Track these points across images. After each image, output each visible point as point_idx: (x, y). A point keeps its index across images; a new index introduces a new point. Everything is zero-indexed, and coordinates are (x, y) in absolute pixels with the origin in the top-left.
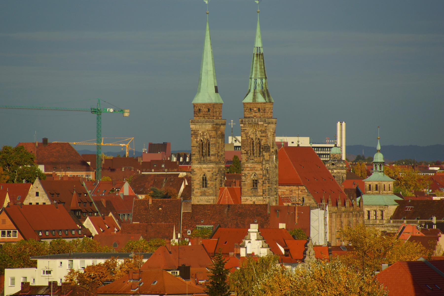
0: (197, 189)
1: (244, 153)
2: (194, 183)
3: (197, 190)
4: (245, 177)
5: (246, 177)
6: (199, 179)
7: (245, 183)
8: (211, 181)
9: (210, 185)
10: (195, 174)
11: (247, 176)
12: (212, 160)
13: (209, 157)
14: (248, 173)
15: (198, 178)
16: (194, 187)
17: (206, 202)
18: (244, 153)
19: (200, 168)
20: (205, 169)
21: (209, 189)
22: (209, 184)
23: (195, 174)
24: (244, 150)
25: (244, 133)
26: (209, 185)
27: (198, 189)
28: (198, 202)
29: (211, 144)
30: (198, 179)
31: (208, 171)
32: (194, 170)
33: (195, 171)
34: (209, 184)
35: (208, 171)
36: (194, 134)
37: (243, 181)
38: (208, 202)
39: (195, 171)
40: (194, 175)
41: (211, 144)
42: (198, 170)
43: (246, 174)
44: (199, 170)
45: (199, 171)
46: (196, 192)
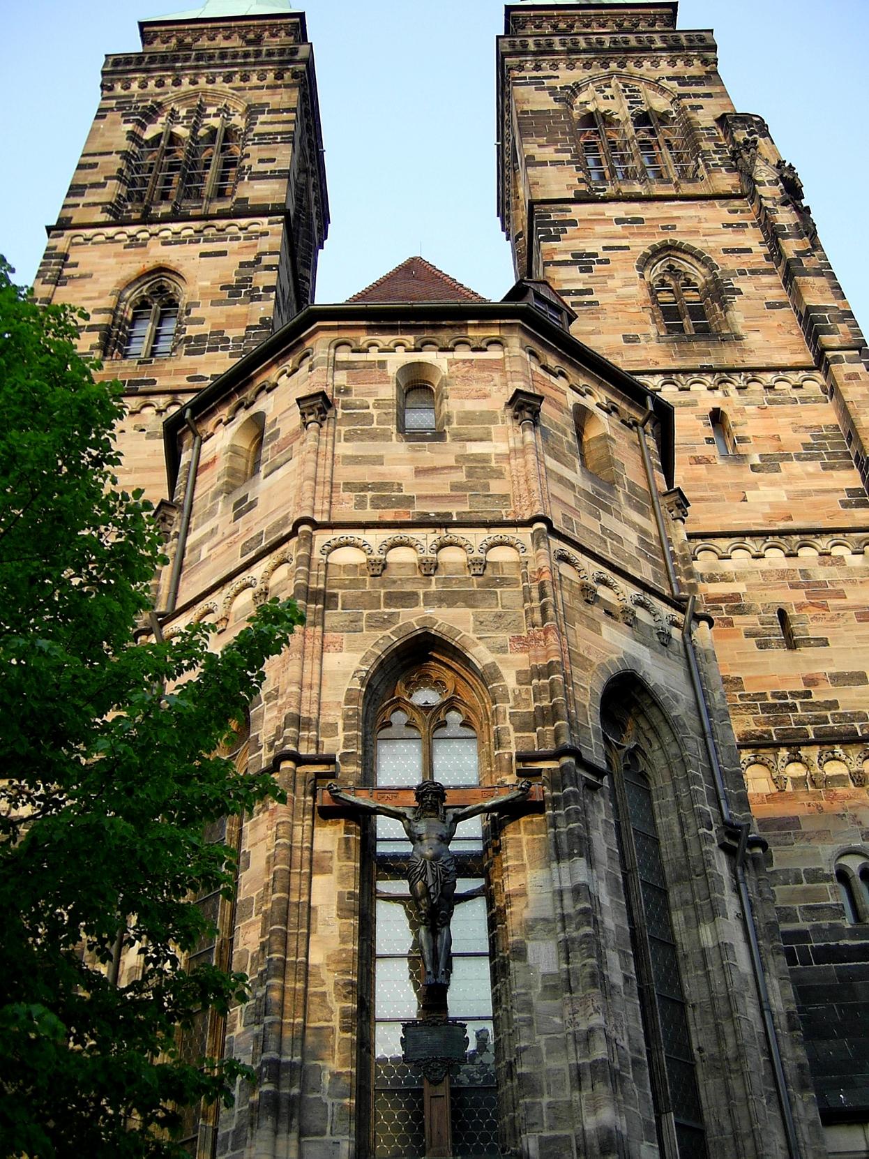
14: (605, 248)
36: (119, 109)
43: (595, 255)
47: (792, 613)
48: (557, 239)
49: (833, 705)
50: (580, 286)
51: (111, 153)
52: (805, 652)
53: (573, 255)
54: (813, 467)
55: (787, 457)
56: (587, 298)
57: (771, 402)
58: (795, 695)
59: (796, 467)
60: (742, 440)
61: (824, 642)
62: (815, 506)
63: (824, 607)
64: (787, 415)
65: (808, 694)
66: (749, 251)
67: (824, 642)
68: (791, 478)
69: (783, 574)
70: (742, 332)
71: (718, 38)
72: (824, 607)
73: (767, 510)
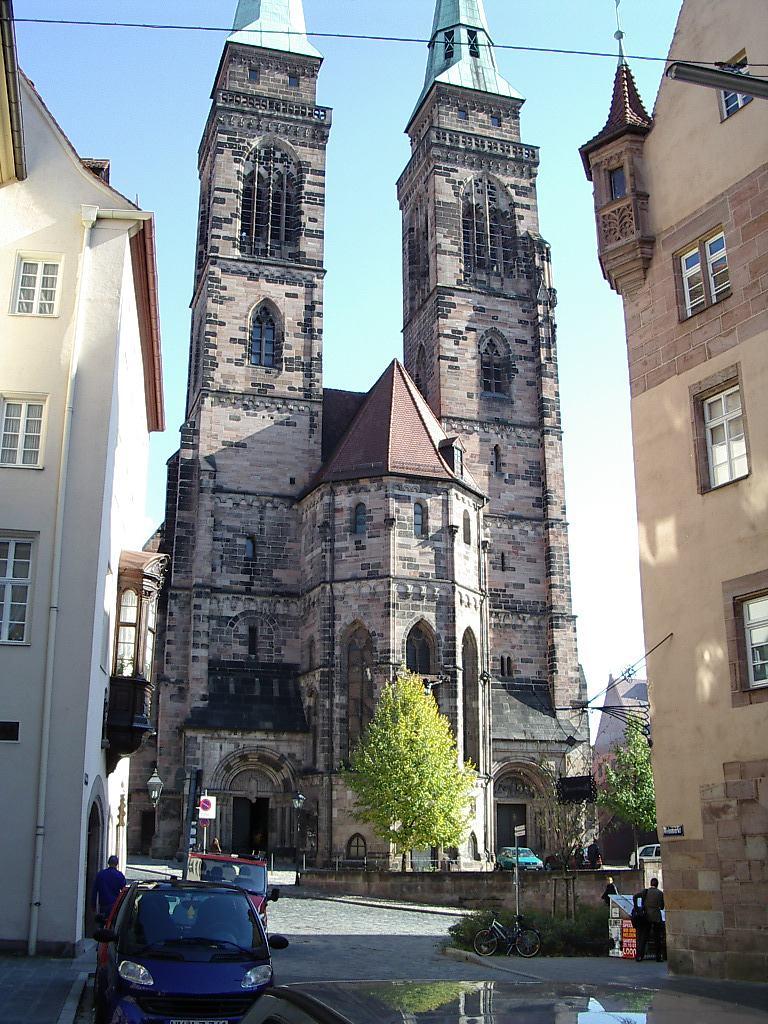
0: (229, 361)
1: (451, 253)
4: (457, 344)
5: (461, 341)
7: (457, 368)
10: (221, 301)
11: (465, 339)
15: (238, 315)
16: (219, 354)
18: (451, 253)
22: (289, 347)
24: (448, 241)
25: (447, 181)
27: (236, 364)
31: (287, 295)
33: (225, 288)
34: (289, 347)
35: (287, 295)
37: (446, 358)
39: (225, 288)
43: (461, 332)
47: (506, 555)
48: (446, 317)
49: (512, 596)
50: (453, 355)
51: (229, 191)
52: (507, 573)
53: (453, 331)
54: (526, 483)
55: (518, 477)
56: (456, 364)
57: (518, 444)
58: (501, 590)
59: (520, 483)
60: (504, 464)
61: (514, 569)
62: (524, 504)
63: (517, 553)
64: (522, 453)
65: (505, 591)
66: (525, 342)
67: (514, 569)
68: (518, 489)
69: (507, 536)
70: (514, 398)
71: (542, 155)
72: (517, 553)
73: (506, 504)
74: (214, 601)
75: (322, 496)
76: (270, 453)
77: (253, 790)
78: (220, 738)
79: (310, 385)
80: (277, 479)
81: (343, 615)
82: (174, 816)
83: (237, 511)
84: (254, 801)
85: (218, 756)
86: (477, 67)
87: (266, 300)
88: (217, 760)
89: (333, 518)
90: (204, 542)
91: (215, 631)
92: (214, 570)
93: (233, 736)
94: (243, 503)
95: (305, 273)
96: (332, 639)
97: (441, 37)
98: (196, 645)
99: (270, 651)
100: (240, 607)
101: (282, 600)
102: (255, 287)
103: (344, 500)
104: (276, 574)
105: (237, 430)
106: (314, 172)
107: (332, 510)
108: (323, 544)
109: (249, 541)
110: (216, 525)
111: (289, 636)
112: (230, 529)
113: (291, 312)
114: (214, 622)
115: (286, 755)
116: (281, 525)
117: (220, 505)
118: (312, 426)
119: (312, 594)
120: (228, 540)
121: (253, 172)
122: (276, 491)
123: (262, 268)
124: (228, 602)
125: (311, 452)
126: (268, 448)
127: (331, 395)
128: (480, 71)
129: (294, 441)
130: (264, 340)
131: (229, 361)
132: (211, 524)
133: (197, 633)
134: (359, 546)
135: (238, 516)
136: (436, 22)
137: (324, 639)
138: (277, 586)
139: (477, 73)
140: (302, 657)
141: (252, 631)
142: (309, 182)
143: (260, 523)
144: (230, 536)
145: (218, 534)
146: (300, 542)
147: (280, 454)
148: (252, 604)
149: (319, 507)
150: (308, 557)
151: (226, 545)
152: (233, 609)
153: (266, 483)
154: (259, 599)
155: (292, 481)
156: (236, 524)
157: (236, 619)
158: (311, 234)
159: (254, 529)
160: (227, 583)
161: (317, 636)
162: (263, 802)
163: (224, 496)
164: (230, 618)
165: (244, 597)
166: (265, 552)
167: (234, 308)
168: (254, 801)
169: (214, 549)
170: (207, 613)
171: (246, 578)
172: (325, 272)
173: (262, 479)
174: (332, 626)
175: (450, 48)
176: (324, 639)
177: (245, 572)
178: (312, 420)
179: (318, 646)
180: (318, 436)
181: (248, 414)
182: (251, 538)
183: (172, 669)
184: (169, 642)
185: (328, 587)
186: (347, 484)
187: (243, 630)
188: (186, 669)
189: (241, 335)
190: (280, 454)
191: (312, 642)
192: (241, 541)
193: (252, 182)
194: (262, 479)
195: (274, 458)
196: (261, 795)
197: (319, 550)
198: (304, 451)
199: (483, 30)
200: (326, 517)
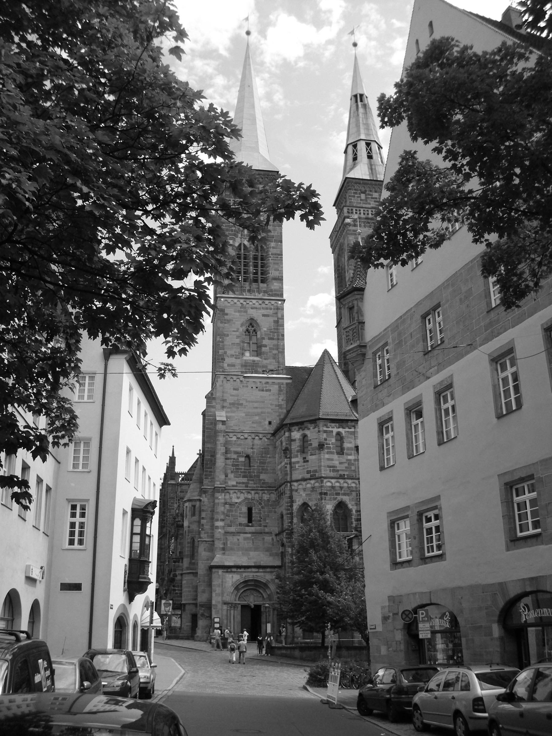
0: (232, 356)
2: (226, 343)
3: (233, 360)
6: (238, 333)
8: (270, 339)
9: (270, 348)
10: (229, 321)
12: (275, 290)
13: (265, 285)
15: (236, 330)
16: (225, 353)
17: (259, 390)
19: (241, 308)
20: (255, 310)
21: (265, 359)
22: (266, 346)
23: (229, 321)
26: (268, 348)
27: (236, 358)
28: (234, 389)
29: (272, 254)
30: (234, 333)
31: (264, 315)
32: (226, 311)
33: (227, 314)
34: (266, 346)
35: (264, 315)
38: (263, 391)
39: (227, 314)
40: (225, 323)
41: (272, 254)
42: (235, 312)
44: (239, 311)
45: (237, 314)
46: (228, 365)
74: (228, 494)
75: (285, 432)
76: (256, 408)
77: (252, 600)
78: (231, 572)
79: (278, 367)
80: (260, 423)
81: (297, 500)
82: (207, 617)
83: (238, 443)
84: (253, 606)
85: (231, 582)
86: (371, 165)
87: (252, 319)
88: (230, 585)
89: (290, 445)
90: (220, 461)
91: (228, 511)
92: (226, 476)
93: (239, 570)
94: (242, 437)
95: (273, 302)
96: (291, 514)
97: (350, 148)
98: (217, 520)
99: (260, 521)
100: (242, 497)
101: (266, 492)
102: (244, 312)
103: (296, 435)
104: (262, 476)
105: (238, 396)
106: (275, 241)
107: (291, 440)
108: (286, 460)
109: (247, 459)
110: (227, 452)
111: (270, 512)
112: (236, 453)
113: (265, 325)
114: (227, 506)
115: (270, 580)
116: (264, 448)
117: (229, 439)
118: (280, 390)
119: (281, 488)
120: (234, 459)
121: (240, 245)
122: (260, 430)
123: (248, 301)
124: (235, 494)
125: (280, 406)
126: (256, 405)
127: (293, 370)
128: (373, 167)
129: (270, 400)
130: (251, 342)
131: (232, 356)
132: (224, 451)
133: (218, 513)
134: (305, 461)
135: (239, 445)
136: (348, 139)
137: (288, 514)
138: (263, 483)
139: (372, 169)
140: (278, 524)
141: (250, 510)
142: (273, 248)
143: (252, 448)
144: (235, 456)
145: (229, 455)
146: (275, 458)
147: (262, 408)
148: (249, 494)
149: (283, 438)
150: (279, 467)
151: (233, 462)
152: (238, 498)
153: (255, 425)
154: (253, 492)
155: (270, 423)
156: (239, 449)
157: (240, 503)
158: (275, 279)
159: (250, 452)
160: (234, 483)
161: (285, 512)
162: (258, 608)
163: (231, 435)
164: (236, 503)
165: (244, 491)
166: (255, 465)
167: (233, 325)
168: (253, 606)
169: (226, 464)
170: (223, 501)
171: (245, 480)
172: (284, 300)
173: (253, 423)
174: (291, 506)
175: (356, 154)
176: (288, 514)
177: (244, 477)
178: (280, 387)
179: (285, 517)
180: (282, 397)
181: (243, 386)
182: (248, 457)
183: (205, 533)
184: (203, 518)
185: (289, 484)
186: (297, 426)
187: (245, 509)
188: (213, 533)
189: (238, 341)
190: (262, 408)
191: (282, 516)
192: (242, 459)
193: (240, 249)
194: (253, 423)
195: (259, 410)
196: (257, 603)
197: (283, 464)
198: (276, 406)
199: (375, 141)
200: (287, 444)
